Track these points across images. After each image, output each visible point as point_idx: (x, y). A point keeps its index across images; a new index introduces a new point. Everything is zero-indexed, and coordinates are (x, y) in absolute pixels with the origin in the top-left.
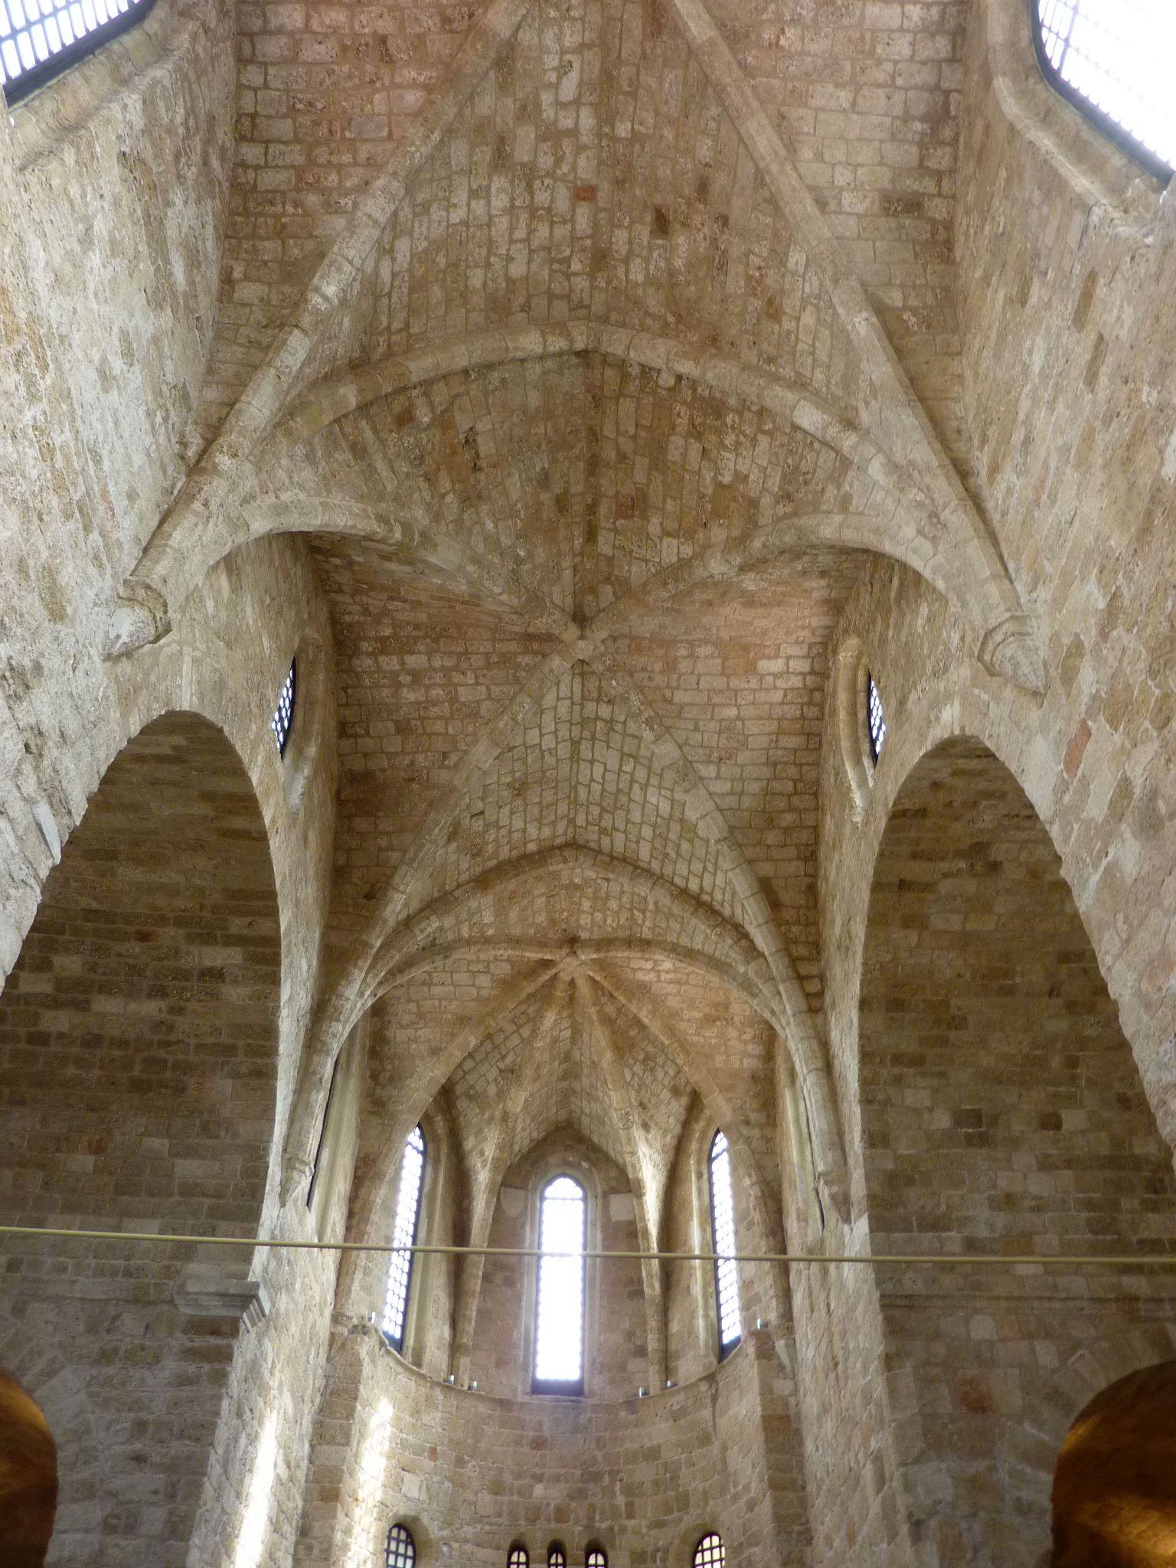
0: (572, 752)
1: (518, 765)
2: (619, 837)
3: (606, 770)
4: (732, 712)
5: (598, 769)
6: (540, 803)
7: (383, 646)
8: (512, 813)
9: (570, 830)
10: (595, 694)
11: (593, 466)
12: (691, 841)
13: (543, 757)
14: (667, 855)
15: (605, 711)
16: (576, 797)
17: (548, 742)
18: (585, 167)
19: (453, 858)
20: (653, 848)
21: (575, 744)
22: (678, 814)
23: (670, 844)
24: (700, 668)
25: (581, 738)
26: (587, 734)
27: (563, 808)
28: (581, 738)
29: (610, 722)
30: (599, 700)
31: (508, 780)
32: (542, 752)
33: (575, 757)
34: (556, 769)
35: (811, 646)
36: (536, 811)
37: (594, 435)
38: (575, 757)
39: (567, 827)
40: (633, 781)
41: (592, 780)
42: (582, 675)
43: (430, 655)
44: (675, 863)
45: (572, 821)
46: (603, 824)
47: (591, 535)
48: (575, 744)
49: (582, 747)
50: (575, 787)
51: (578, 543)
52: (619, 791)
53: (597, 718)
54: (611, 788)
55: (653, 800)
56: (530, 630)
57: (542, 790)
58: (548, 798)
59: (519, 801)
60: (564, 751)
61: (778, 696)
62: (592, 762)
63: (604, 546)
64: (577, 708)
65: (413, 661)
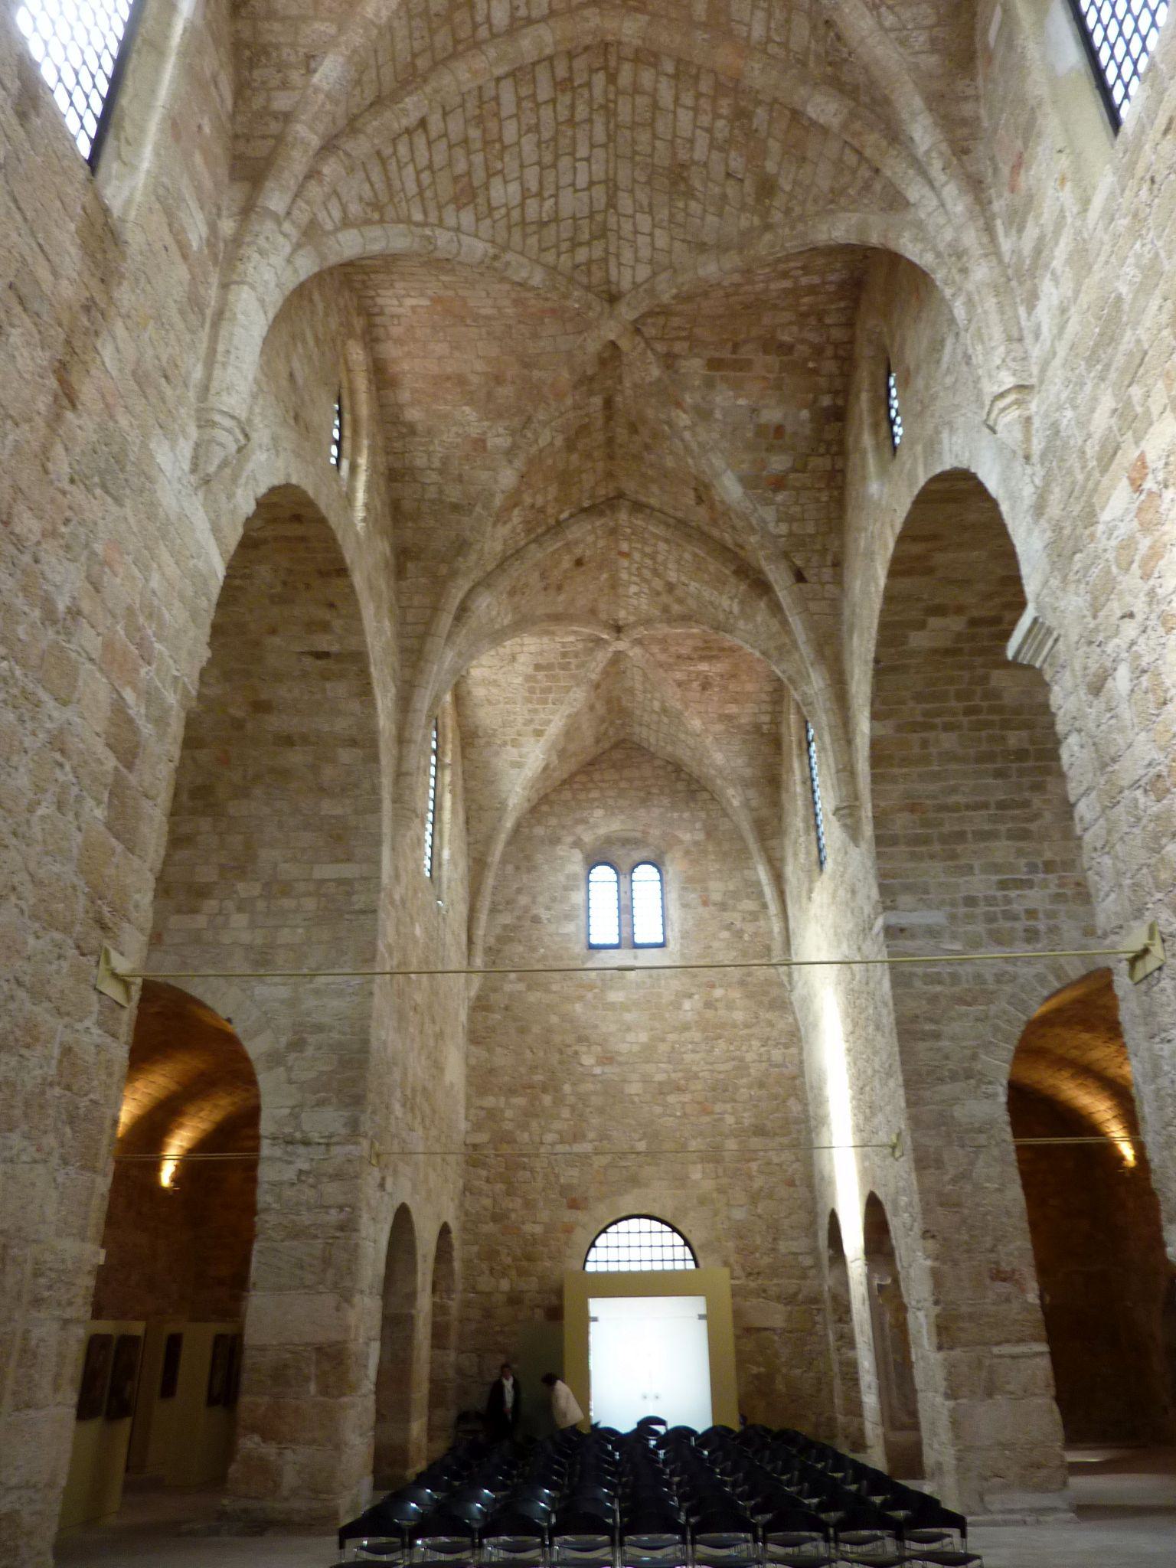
0: (615, 195)
1: (680, 217)
2: (544, 93)
3: (573, 185)
4: (443, 278)
5: (582, 181)
6: (655, 137)
7: (812, 290)
8: (691, 141)
9: (613, 63)
10: (594, 267)
11: (610, 441)
12: (456, 179)
13: (650, 205)
14: (480, 120)
15: (582, 255)
16: (608, 123)
17: (644, 222)
18: (625, 563)
19: (774, 146)
20: (497, 115)
21: (612, 204)
22: (481, 200)
23: (478, 145)
24: (490, 302)
25: (605, 211)
26: (599, 218)
27: (624, 109)
28: (605, 211)
29: (575, 244)
30: (590, 262)
31: (693, 204)
32: (651, 213)
33: (612, 187)
34: (634, 181)
35: (381, 313)
36: (660, 127)
37: (611, 457)
38: (612, 187)
39: (617, 70)
40: (539, 194)
41: (588, 159)
42: (609, 282)
43: (766, 290)
44: (466, 122)
45: (612, 78)
46: (566, 99)
47: (608, 403)
48: (612, 204)
49: (604, 200)
50: (609, 136)
51: (619, 399)
52: (554, 166)
53: (589, 243)
54: (565, 162)
55: (514, 188)
56: (661, 320)
57: (651, 156)
58: (644, 137)
59: (683, 156)
60: (625, 202)
61: (397, 285)
62: (591, 183)
63: (597, 401)
64: (612, 250)
65: (787, 284)
